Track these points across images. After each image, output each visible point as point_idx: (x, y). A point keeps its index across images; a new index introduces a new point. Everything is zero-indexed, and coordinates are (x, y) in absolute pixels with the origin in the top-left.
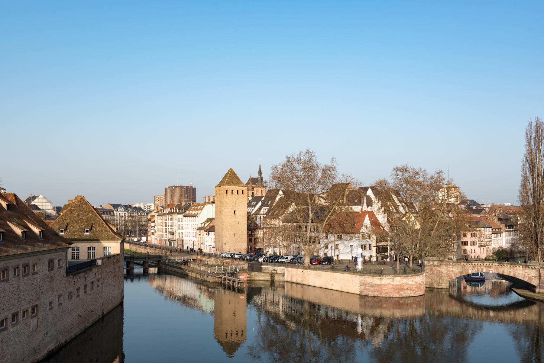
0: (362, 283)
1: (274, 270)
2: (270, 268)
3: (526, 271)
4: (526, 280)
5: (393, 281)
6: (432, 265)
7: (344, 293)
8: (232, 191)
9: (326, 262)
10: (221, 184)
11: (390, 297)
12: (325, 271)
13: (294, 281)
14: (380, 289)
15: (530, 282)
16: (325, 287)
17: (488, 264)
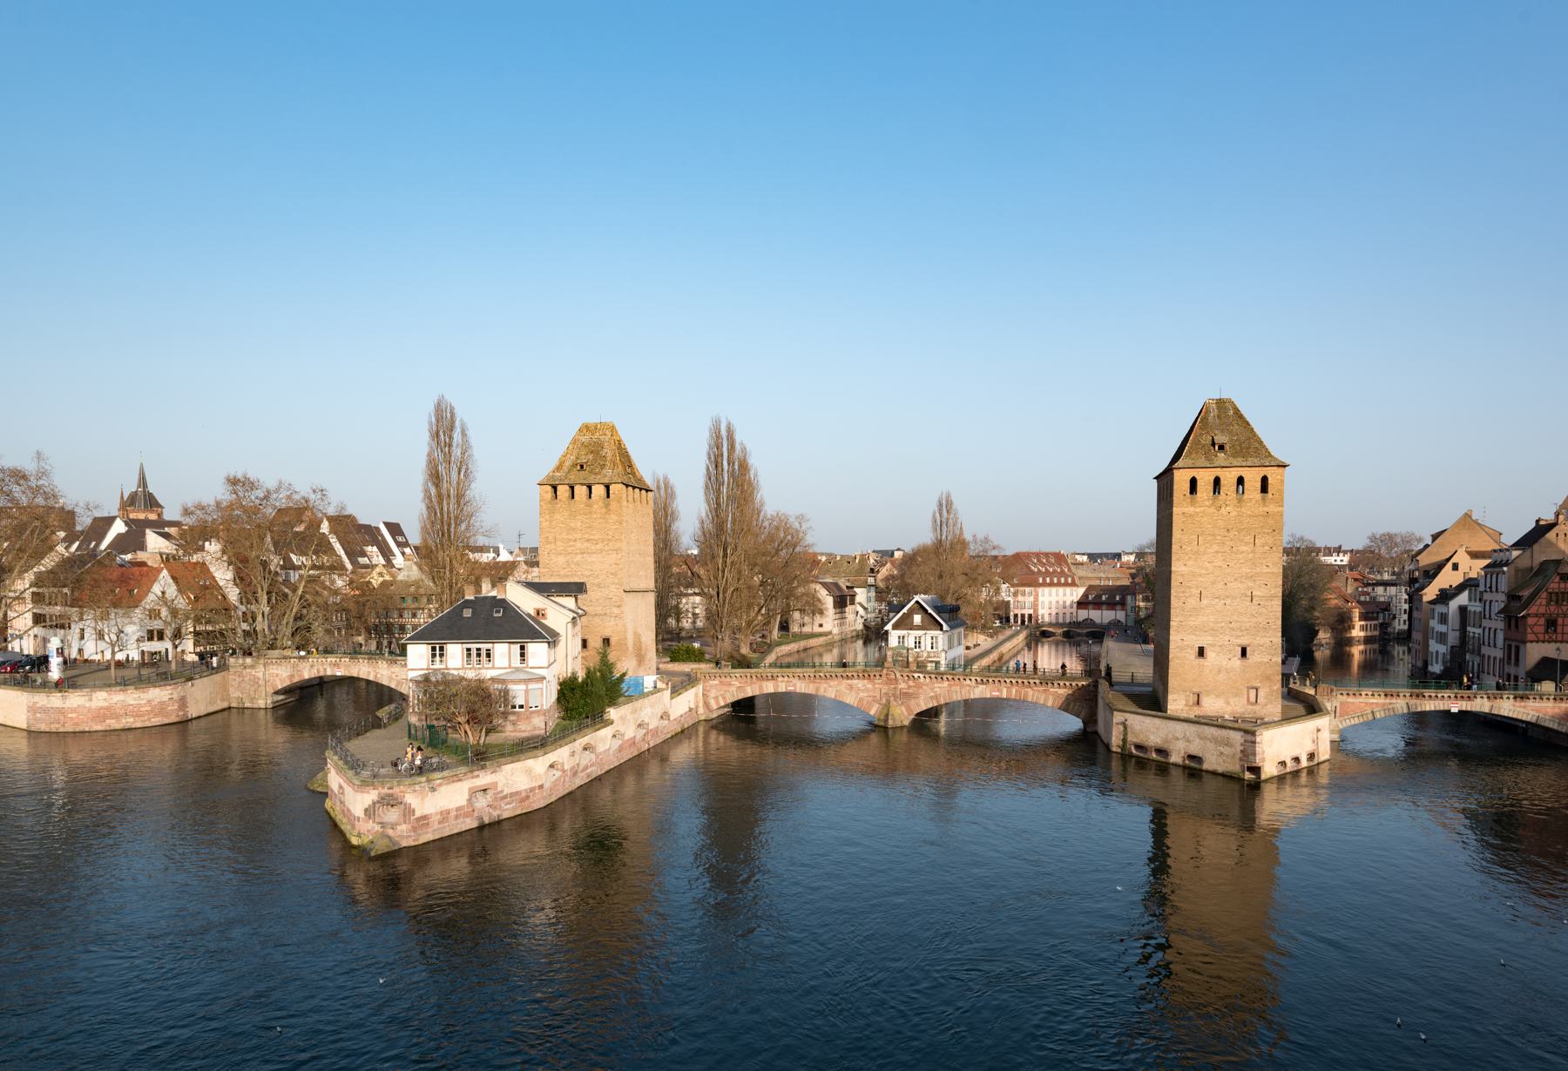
3: (393, 670)
4: (393, 686)
6: (242, 665)
9: (27, 668)
11: (84, 732)
14: (62, 718)
15: (398, 689)
17: (333, 660)
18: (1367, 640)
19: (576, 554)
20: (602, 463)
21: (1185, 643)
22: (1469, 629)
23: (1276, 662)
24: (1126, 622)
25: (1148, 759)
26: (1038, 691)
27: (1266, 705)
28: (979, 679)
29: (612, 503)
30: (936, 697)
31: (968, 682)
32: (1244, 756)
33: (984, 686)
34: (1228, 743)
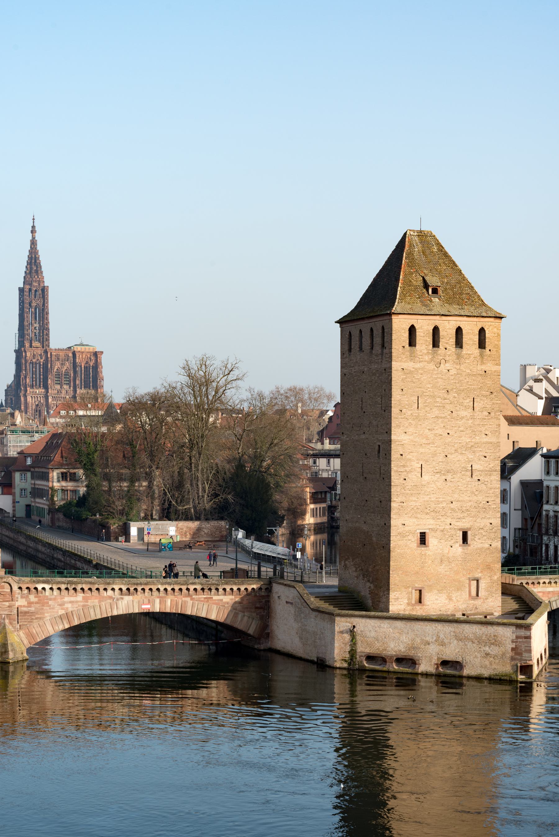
18: (318, 529)
21: (407, 528)
22: (546, 507)
23: (496, 548)
24: (14, 511)
25: (388, 672)
26: (199, 600)
27: (487, 599)
28: (124, 588)
30: (68, 616)
31: (110, 592)
32: (516, 654)
33: (131, 598)
34: (495, 642)
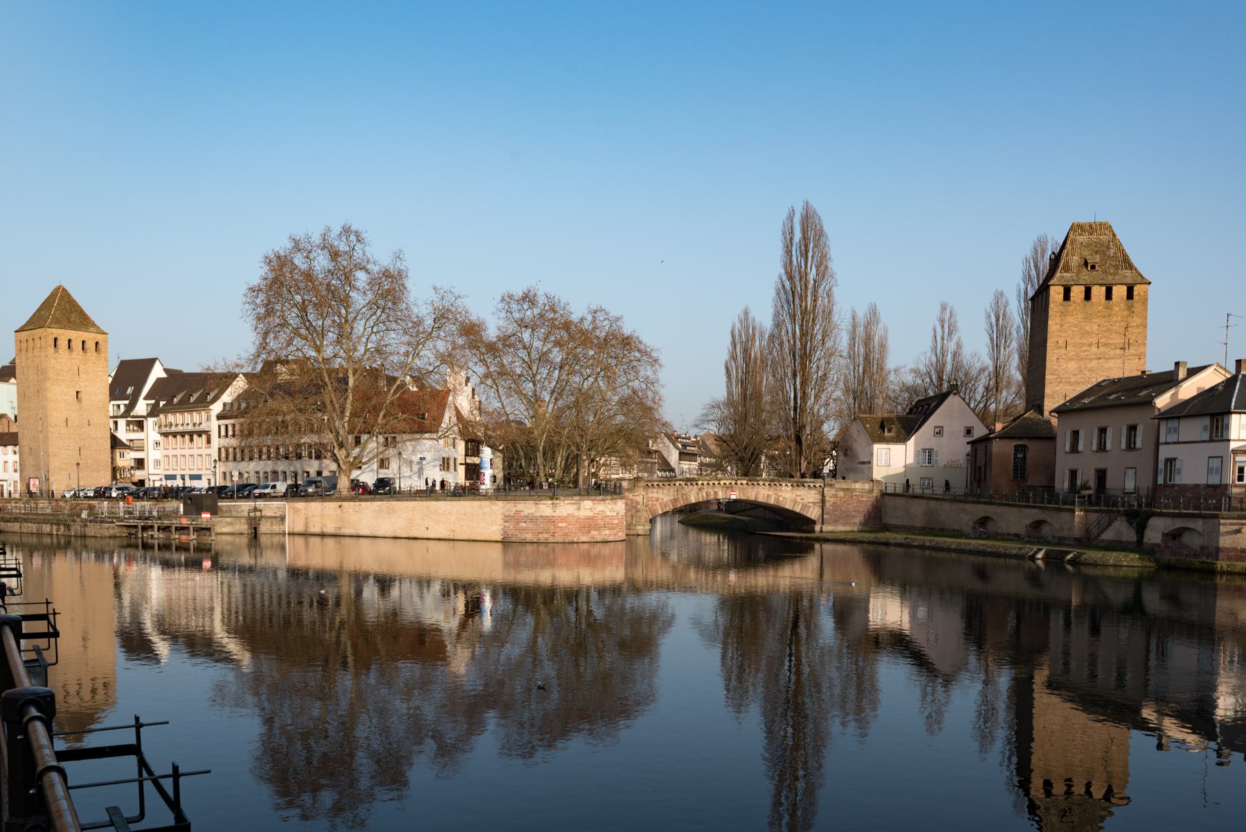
0: (508, 516)
1: (255, 509)
2: (245, 506)
3: (798, 493)
4: (797, 509)
5: (579, 509)
7: (459, 542)
8: (70, 341)
10: (36, 322)
12: (407, 500)
13: (316, 529)
15: (805, 514)
16: (407, 536)
17: (727, 482)
19: (1091, 360)
20: (1113, 263)
29: (1136, 305)
